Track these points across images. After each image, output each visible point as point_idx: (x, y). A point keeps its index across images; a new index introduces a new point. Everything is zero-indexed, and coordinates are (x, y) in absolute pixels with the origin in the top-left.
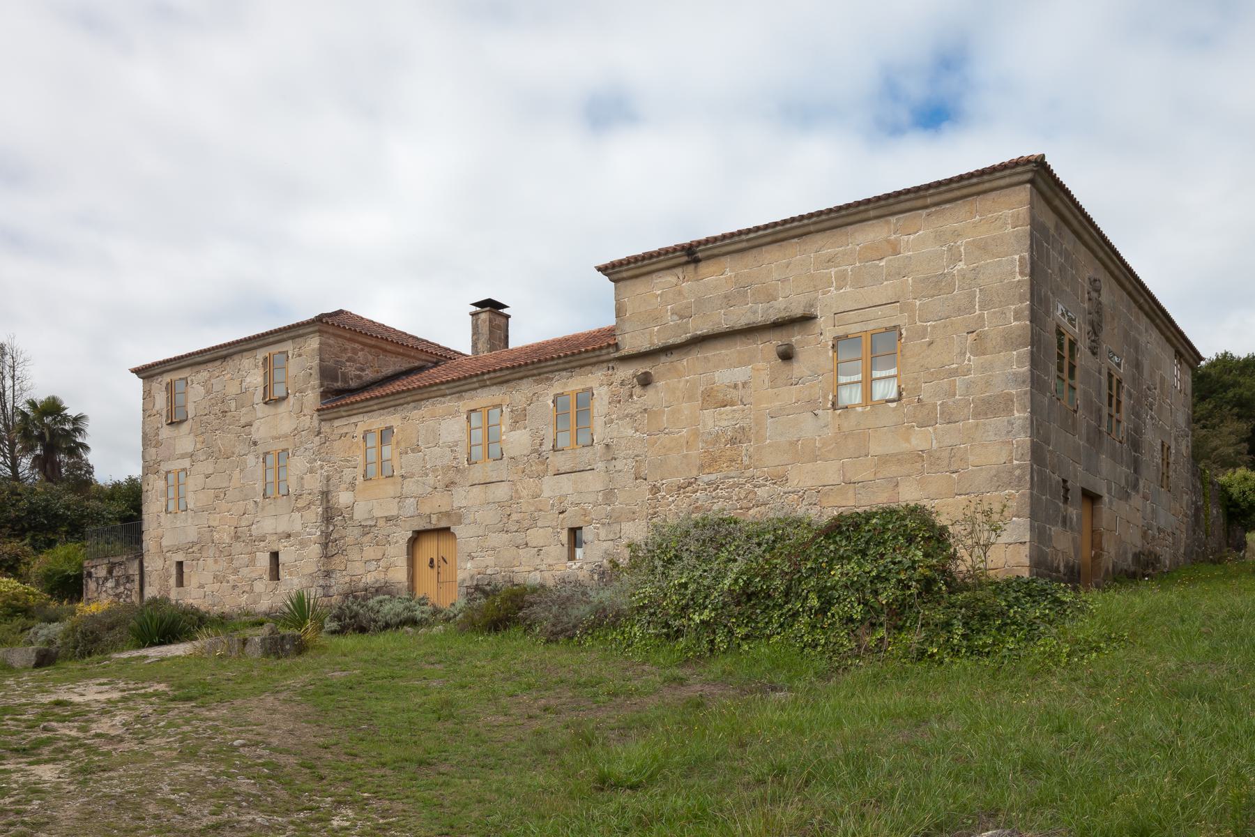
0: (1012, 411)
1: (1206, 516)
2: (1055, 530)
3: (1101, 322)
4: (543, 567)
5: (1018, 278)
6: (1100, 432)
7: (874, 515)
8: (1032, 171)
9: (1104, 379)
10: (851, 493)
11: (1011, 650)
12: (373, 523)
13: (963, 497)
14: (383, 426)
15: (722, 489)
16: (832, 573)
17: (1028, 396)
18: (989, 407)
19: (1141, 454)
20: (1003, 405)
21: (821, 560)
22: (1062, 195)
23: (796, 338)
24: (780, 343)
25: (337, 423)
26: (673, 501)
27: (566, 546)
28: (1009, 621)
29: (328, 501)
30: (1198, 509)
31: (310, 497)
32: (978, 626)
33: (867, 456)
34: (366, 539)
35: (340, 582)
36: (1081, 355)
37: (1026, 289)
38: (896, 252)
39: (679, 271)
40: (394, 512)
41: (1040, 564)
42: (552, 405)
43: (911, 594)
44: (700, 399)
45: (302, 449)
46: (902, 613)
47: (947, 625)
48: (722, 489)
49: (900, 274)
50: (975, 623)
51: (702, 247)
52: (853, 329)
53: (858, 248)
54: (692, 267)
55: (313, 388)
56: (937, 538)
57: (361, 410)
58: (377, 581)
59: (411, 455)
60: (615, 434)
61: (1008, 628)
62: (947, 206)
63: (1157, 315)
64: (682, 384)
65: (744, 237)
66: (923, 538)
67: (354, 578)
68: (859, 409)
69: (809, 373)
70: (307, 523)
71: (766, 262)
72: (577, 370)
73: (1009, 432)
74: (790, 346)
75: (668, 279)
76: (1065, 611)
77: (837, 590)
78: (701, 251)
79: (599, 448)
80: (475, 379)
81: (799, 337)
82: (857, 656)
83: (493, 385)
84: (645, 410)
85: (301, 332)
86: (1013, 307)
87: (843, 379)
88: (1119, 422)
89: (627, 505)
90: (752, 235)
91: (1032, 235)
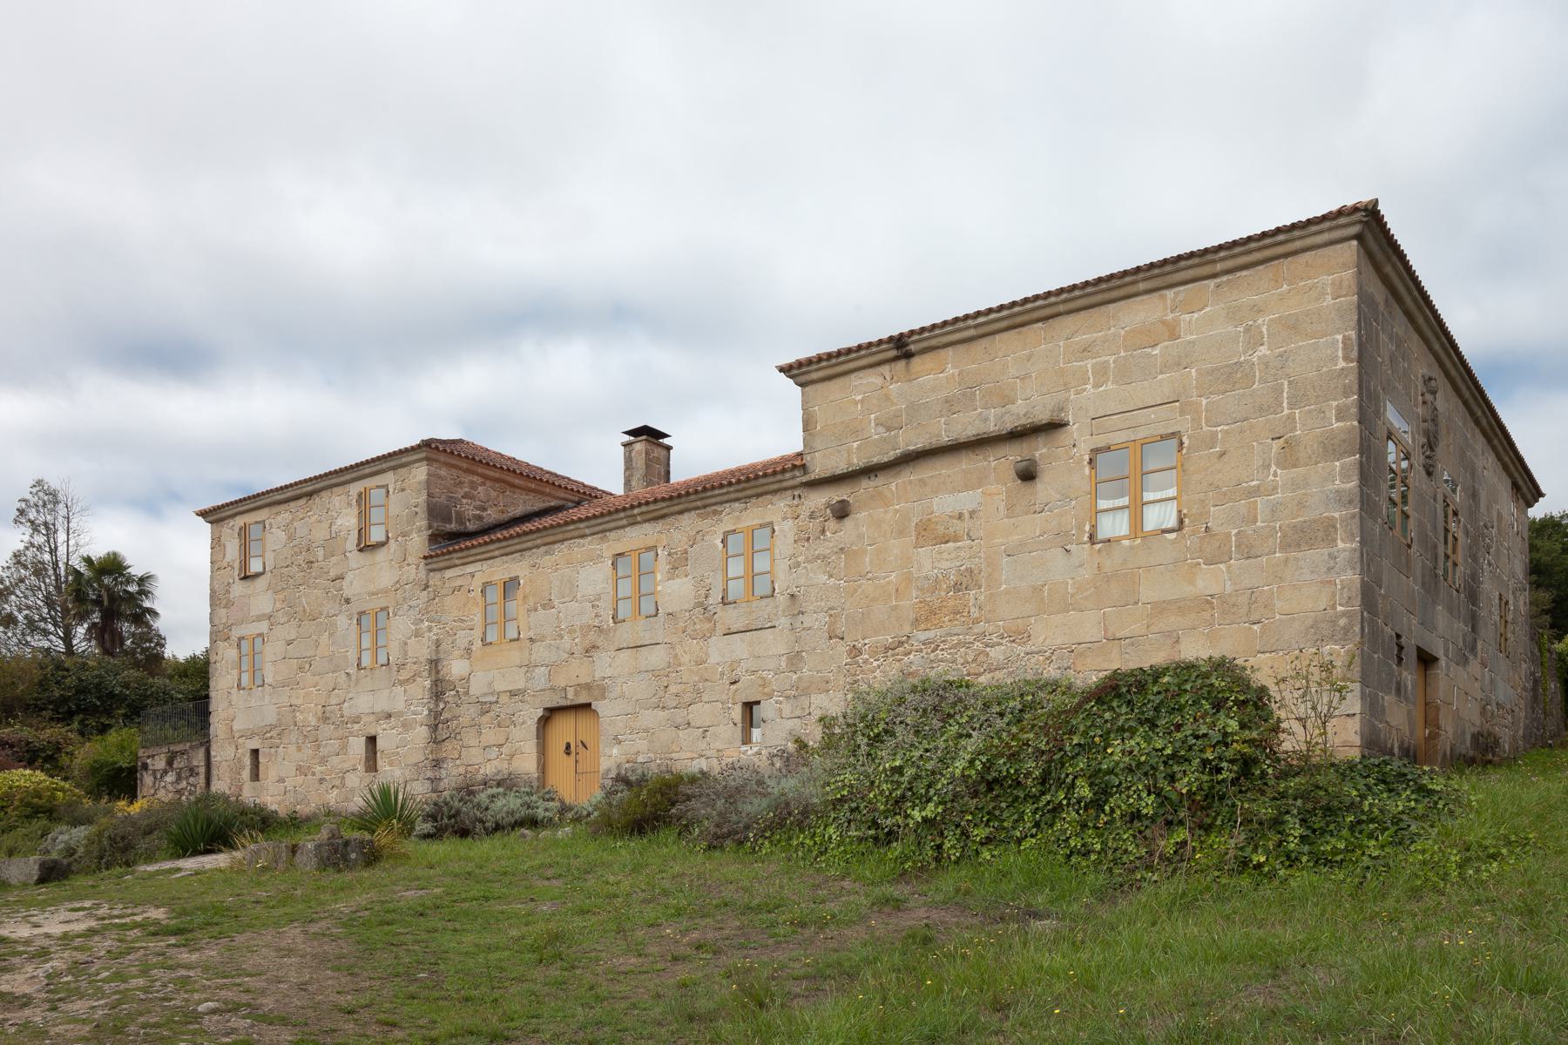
0: (1335, 540)
1: (1544, 690)
2: (1388, 699)
3: (1437, 432)
4: (708, 753)
5: (1342, 364)
6: (1436, 576)
7: (1164, 671)
8: (1361, 222)
9: (1440, 507)
10: (1115, 651)
11: (1376, 858)
12: (494, 699)
13: (1268, 655)
14: (506, 576)
15: (942, 650)
16: (1109, 751)
17: (1357, 520)
18: (1302, 537)
19: (1479, 607)
20: (1327, 531)
21: (1093, 734)
22: (1394, 258)
23: (1039, 449)
24: (1019, 459)
25: (449, 573)
26: (879, 667)
27: (740, 725)
28: (1364, 818)
29: (438, 672)
30: (1536, 681)
31: (415, 667)
32: (1322, 824)
33: (1136, 603)
34: (486, 718)
35: (452, 775)
36: (1415, 474)
37: (1352, 379)
38: (1173, 335)
39: (885, 369)
40: (521, 685)
41: (1371, 742)
42: (721, 545)
43: (1223, 780)
44: (914, 533)
45: (406, 607)
46: (1210, 807)
47: (1277, 823)
48: (942, 650)
49: (1180, 364)
50: (1317, 821)
51: (915, 337)
52: (1118, 438)
53: (1123, 332)
54: (901, 364)
55: (420, 531)
56: (1255, 704)
57: (478, 557)
58: (499, 772)
59: (541, 611)
60: (802, 581)
61: (1364, 826)
62: (1244, 273)
63: (1496, 435)
64: (890, 515)
65: (970, 322)
66: (1236, 702)
67: (470, 769)
68: (1126, 543)
69: (1058, 496)
70: (412, 700)
71: (1000, 354)
72: (754, 500)
73: (1329, 569)
74: (1032, 462)
75: (871, 379)
76: (1436, 803)
77: (1116, 775)
78: (914, 342)
79: (782, 599)
80: (622, 515)
81: (1044, 451)
82: (1149, 868)
83: (648, 521)
84: (842, 549)
85: (404, 460)
86: (1335, 403)
87: (1103, 504)
88: (1455, 565)
89: (818, 672)
90: (981, 320)
91: (1359, 307)
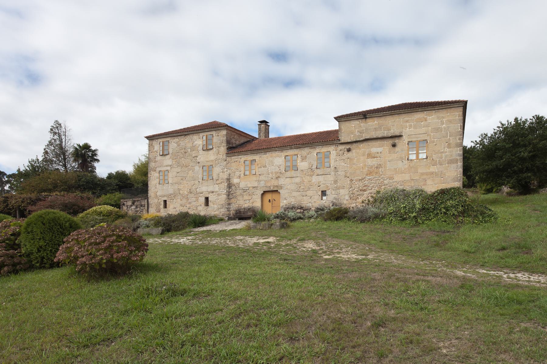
14: (252, 159)
18: (451, 162)
23: (397, 141)
25: (233, 158)
27: (321, 196)
31: (222, 180)
45: (219, 165)
54: (364, 119)
59: (263, 168)
60: (338, 164)
64: (360, 152)
68: (415, 161)
70: (222, 189)
79: (332, 168)
80: (289, 147)
81: (397, 141)
84: (348, 158)
87: (410, 153)
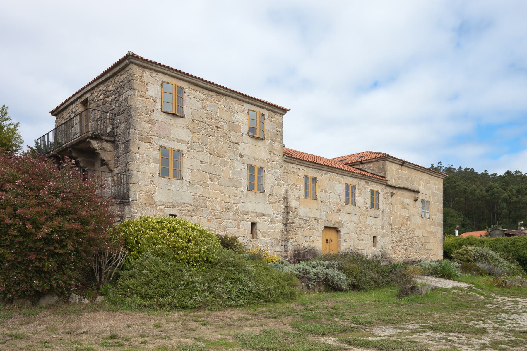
29: (287, 203)
57: (305, 165)
85: (276, 110)
